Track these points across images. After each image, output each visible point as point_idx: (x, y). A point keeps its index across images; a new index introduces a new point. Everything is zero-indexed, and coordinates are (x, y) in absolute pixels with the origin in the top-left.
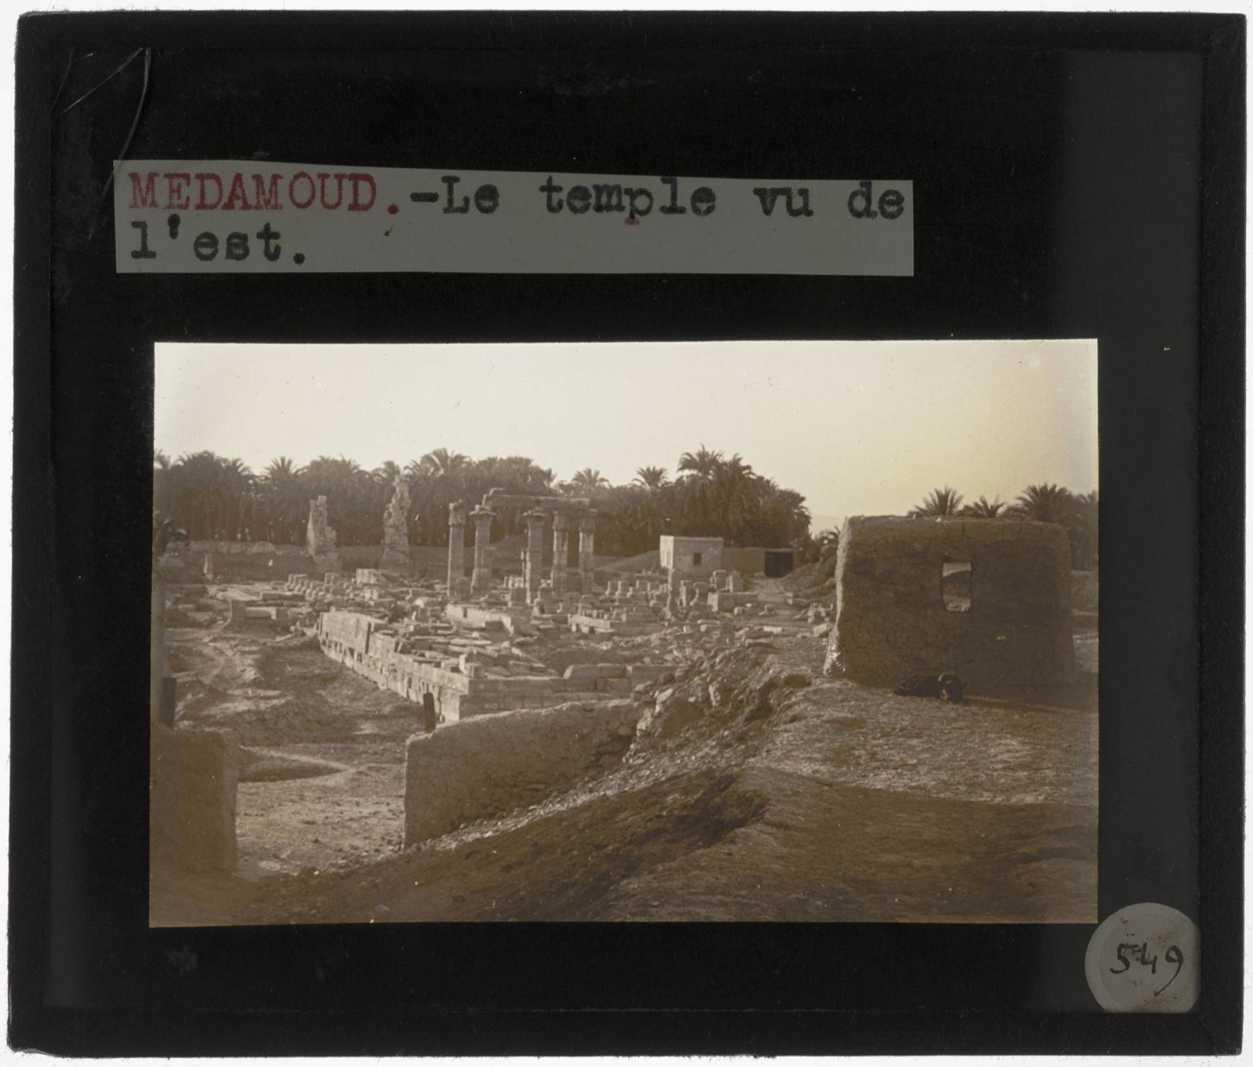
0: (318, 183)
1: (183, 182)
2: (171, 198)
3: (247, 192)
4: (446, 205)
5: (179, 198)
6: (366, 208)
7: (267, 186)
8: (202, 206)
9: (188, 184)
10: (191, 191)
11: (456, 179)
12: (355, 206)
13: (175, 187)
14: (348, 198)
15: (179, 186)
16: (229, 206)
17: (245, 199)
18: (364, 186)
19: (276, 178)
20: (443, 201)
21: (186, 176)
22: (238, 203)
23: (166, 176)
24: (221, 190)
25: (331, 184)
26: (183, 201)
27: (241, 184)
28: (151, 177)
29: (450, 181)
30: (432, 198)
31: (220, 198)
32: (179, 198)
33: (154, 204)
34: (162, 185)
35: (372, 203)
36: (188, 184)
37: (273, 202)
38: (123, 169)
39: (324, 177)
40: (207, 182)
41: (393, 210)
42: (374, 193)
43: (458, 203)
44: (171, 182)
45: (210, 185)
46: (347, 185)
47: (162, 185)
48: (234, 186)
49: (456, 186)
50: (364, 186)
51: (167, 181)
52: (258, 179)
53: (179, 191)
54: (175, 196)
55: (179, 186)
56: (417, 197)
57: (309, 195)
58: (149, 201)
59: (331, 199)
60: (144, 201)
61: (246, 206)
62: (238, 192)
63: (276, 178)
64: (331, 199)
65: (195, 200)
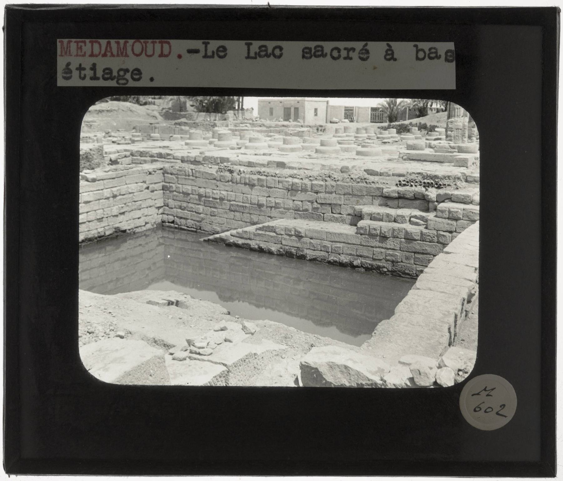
0: (144, 45)
1: (83, 44)
4: (203, 54)
6: (166, 56)
7: (122, 45)
8: (92, 55)
9: (85, 46)
11: (209, 43)
15: (81, 46)
16: (105, 55)
17: (112, 53)
19: (125, 43)
20: (202, 53)
21: (85, 43)
22: (109, 54)
23: (75, 42)
24: (100, 49)
25: (150, 46)
26: (83, 53)
27: (110, 44)
28: (69, 42)
29: (206, 44)
30: (197, 51)
31: (100, 53)
34: (73, 46)
36: (85, 46)
37: (124, 54)
38: (58, 40)
39: (146, 43)
40: (94, 44)
41: (180, 56)
43: (210, 53)
44: (78, 45)
45: (96, 46)
46: (158, 46)
47: (73, 46)
49: (209, 46)
50: (166, 46)
51: (76, 44)
52: (118, 43)
54: (79, 51)
56: (190, 51)
57: (141, 50)
58: (68, 52)
59: (150, 52)
60: (66, 53)
61: (112, 55)
62: (109, 49)
63: (125, 43)
65: (89, 53)
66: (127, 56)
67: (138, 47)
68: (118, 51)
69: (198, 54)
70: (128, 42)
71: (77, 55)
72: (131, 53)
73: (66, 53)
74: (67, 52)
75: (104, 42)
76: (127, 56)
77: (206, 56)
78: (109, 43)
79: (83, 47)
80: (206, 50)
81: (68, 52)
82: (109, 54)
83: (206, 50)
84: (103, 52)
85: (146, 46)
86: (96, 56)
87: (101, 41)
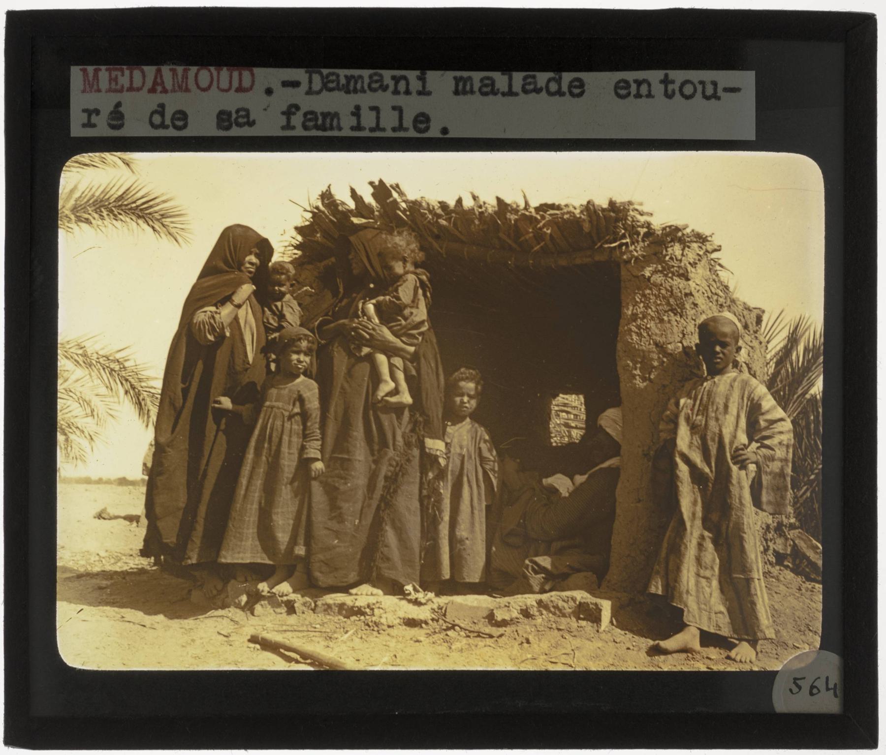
0: (215, 73)
1: (119, 73)
2: (110, 84)
3: (165, 81)
5: (117, 84)
8: (131, 89)
9: (123, 75)
10: (124, 81)
12: (240, 89)
13: (113, 76)
14: (235, 84)
15: (117, 76)
16: (152, 90)
18: (246, 74)
20: (304, 87)
22: (159, 88)
26: (119, 87)
30: (295, 84)
32: (117, 84)
33: (99, 91)
35: (251, 88)
41: (269, 92)
42: (253, 82)
44: (110, 76)
45: (137, 74)
46: (236, 74)
48: (156, 78)
51: (107, 74)
52: (174, 71)
53: (116, 80)
54: (113, 84)
55: (117, 76)
58: (95, 87)
61: (165, 91)
62: (159, 80)
64: (224, 84)
65: (127, 85)
66: (187, 90)
67: (204, 76)
68: (173, 85)
69: (296, 89)
70: (189, 70)
71: (110, 90)
72: (195, 87)
73: (91, 86)
74: (91, 86)
75: (150, 70)
76: (187, 90)
77: (309, 92)
78: (159, 71)
79: (119, 77)
80: (310, 82)
81: (95, 87)
82: (159, 88)
83: (310, 82)
84: (149, 83)
85: (219, 73)
86: (139, 89)
87: (146, 68)
